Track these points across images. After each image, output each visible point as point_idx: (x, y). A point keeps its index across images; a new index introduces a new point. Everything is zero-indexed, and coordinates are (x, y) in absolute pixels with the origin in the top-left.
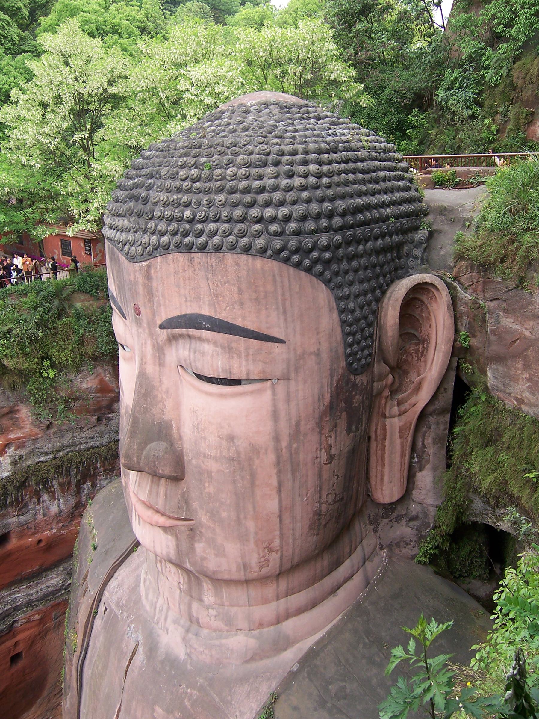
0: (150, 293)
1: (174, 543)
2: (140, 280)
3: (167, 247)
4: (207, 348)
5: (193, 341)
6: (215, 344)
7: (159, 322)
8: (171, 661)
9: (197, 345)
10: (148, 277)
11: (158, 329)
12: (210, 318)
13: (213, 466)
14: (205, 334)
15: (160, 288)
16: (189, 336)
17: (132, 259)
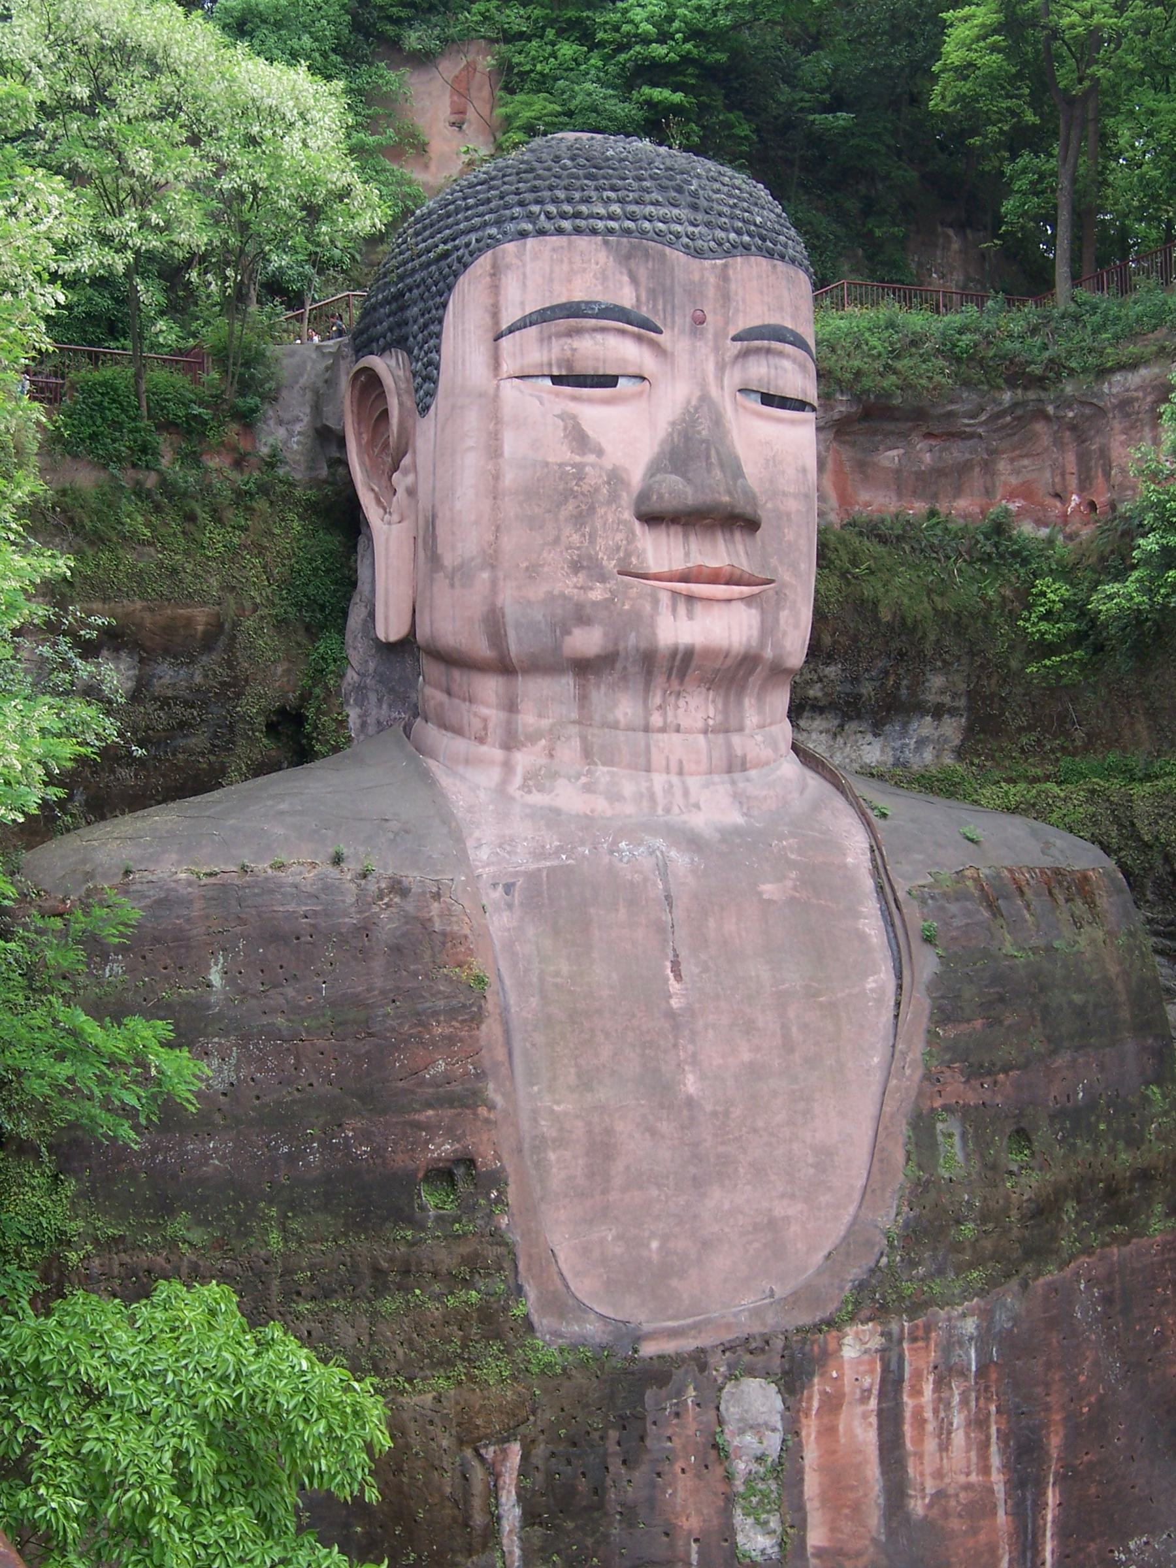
0: (725, 298)
1: (758, 618)
2: (712, 280)
3: (746, 247)
4: (787, 364)
5: (770, 358)
6: (794, 361)
7: (732, 332)
8: (729, 835)
9: (774, 360)
10: (724, 277)
11: (729, 342)
12: (792, 331)
13: (792, 505)
14: (788, 348)
15: (740, 291)
16: (768, 351)
17: (698, 254)
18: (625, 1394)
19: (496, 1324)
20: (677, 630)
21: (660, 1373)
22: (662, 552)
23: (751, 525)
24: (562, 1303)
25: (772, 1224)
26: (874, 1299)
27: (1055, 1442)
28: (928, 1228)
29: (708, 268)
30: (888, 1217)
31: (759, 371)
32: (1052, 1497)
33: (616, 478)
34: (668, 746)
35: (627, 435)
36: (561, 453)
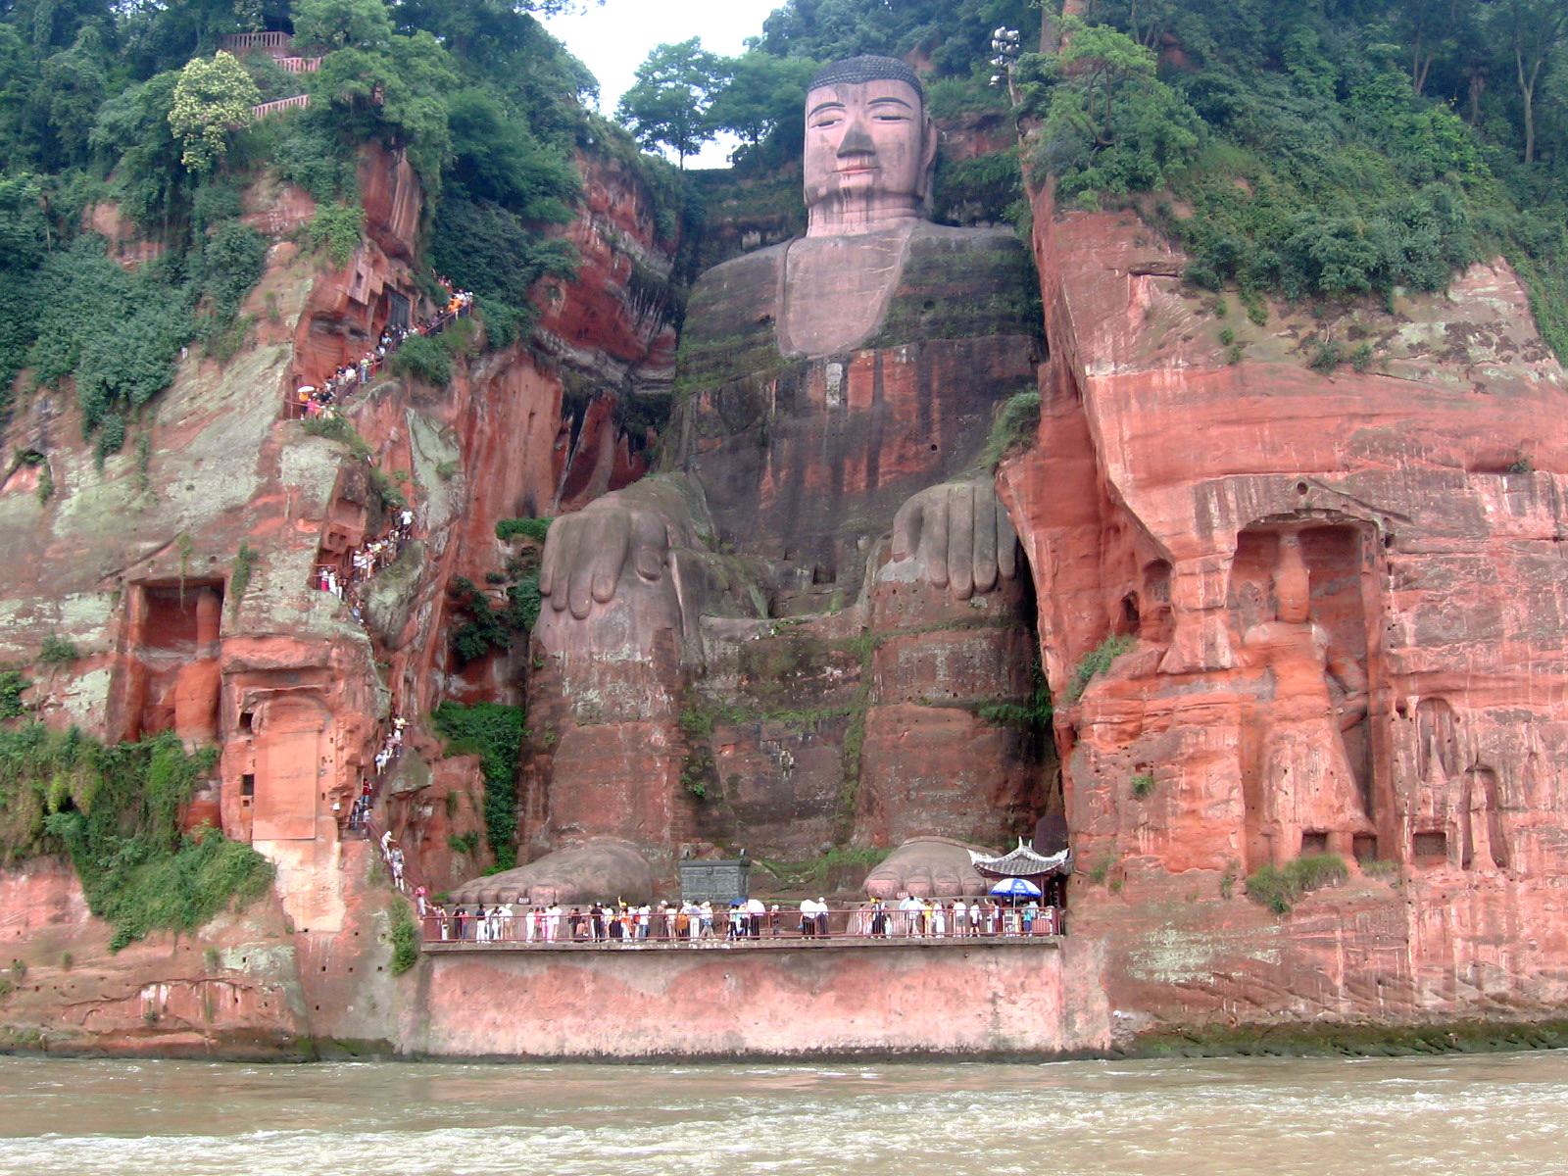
18: (804, 367)
19: (772, 355)
20: (844, 183)
21: (811, 363)
22: (842, 164)
23: (871, 153)
24: (789, 347)
25: (849, 328)
26: (871, 344)
27: (935, 385)
28: (891, 326)
29: (860, 87)
30: (881, 322)
31: (880, 111)
32: (936, 402)
33: (832, 148)
34: (846, 216)
35: (836, 136)
36: (819, 144)
